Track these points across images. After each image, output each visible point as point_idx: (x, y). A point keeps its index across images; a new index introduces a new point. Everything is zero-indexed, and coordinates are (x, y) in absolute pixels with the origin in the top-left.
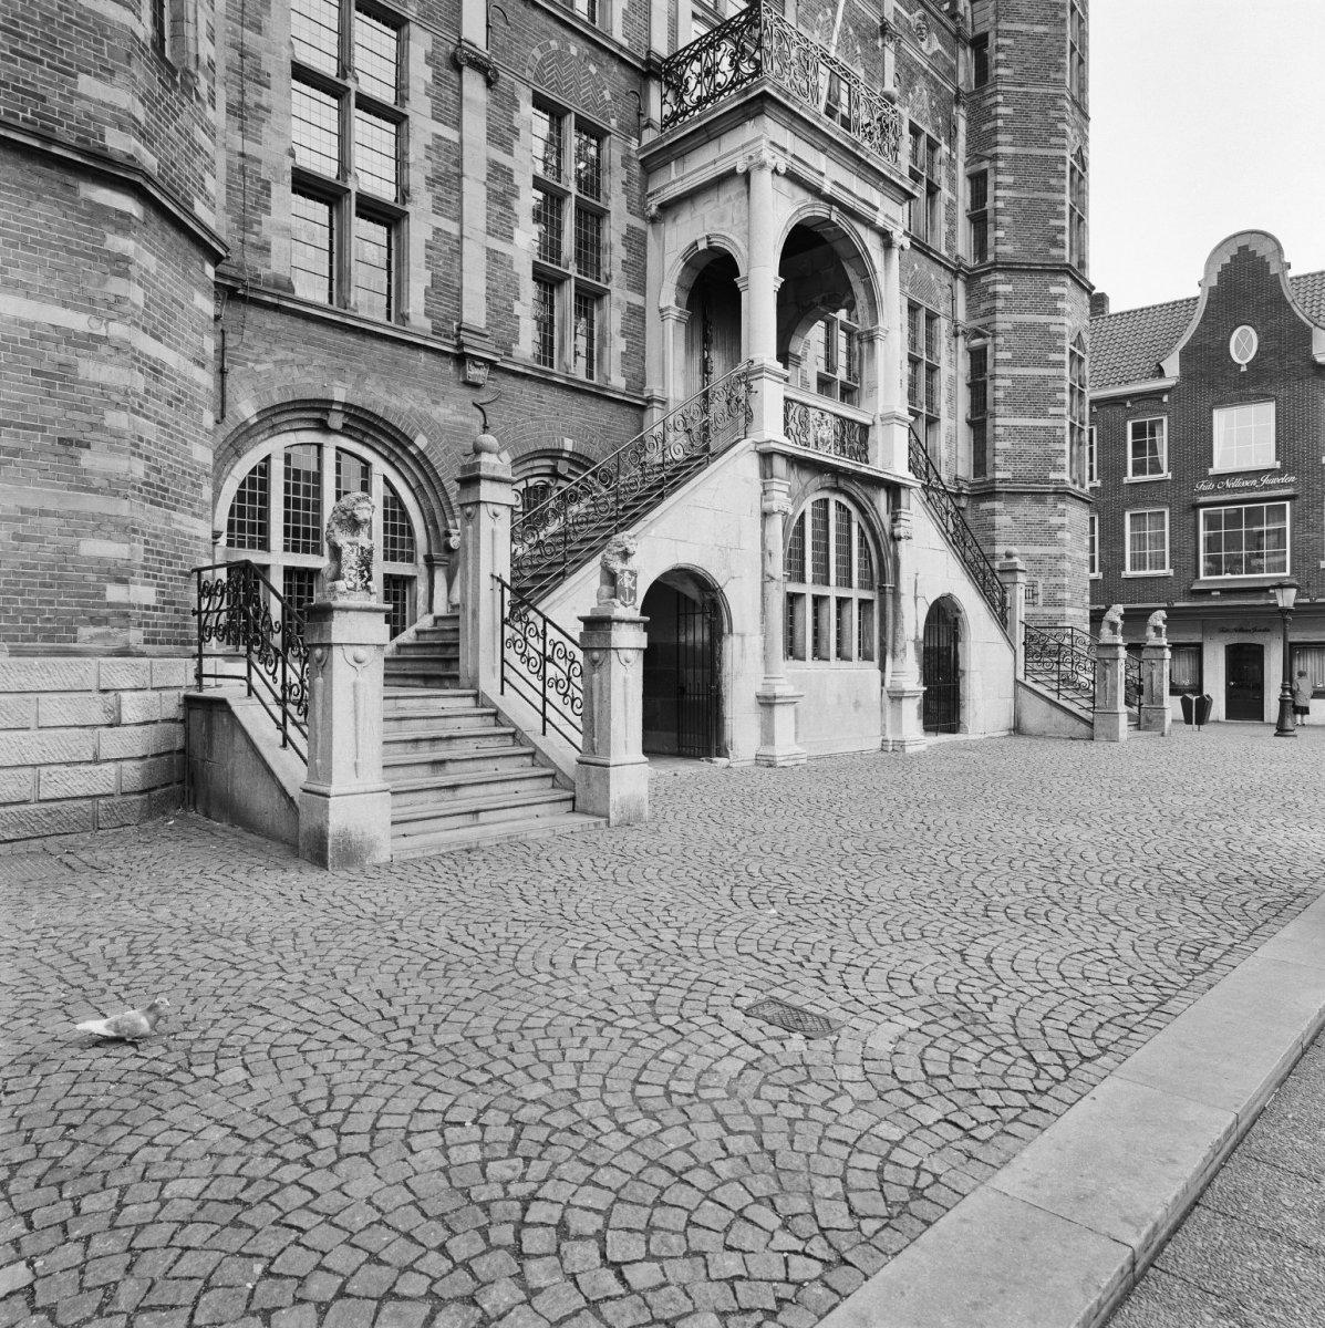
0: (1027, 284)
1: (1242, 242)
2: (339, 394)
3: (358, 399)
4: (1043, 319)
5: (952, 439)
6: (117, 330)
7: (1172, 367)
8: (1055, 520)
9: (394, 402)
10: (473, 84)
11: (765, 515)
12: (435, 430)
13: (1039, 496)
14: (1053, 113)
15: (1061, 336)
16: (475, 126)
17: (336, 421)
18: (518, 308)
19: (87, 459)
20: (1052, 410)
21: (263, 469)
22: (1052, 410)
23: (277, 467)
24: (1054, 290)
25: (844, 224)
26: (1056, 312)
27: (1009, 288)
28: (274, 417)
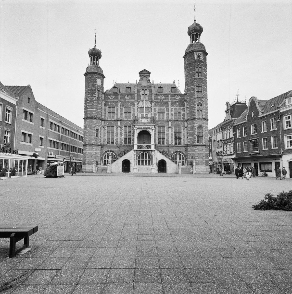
0: (191, 121)
1: (252, 98)
2: (109, 150)
3: (111, 150)
4: (193, 125)
5: (184, 140)
6: (93, 151)
7: (246, 118)
8: (195, 149)
9: (113, 150)
10: (119, 128)
11: (134, 155)
12: (116, 151)
13: (193, 146)
14: (194, 101)
15: (195, 127)
16: (119, 131)
17: (110, 151)
18: (122, 142)
19: (92, 157)
20: (194, 136)
21: (106, 154)
22: (194, 136)
23: (107, 154)
24: (194, 121)
25: (146, 130)
26: (194, 124)
27: (189, 122)
28: (106, 152)
